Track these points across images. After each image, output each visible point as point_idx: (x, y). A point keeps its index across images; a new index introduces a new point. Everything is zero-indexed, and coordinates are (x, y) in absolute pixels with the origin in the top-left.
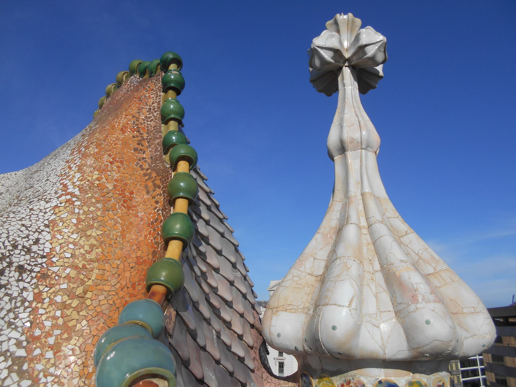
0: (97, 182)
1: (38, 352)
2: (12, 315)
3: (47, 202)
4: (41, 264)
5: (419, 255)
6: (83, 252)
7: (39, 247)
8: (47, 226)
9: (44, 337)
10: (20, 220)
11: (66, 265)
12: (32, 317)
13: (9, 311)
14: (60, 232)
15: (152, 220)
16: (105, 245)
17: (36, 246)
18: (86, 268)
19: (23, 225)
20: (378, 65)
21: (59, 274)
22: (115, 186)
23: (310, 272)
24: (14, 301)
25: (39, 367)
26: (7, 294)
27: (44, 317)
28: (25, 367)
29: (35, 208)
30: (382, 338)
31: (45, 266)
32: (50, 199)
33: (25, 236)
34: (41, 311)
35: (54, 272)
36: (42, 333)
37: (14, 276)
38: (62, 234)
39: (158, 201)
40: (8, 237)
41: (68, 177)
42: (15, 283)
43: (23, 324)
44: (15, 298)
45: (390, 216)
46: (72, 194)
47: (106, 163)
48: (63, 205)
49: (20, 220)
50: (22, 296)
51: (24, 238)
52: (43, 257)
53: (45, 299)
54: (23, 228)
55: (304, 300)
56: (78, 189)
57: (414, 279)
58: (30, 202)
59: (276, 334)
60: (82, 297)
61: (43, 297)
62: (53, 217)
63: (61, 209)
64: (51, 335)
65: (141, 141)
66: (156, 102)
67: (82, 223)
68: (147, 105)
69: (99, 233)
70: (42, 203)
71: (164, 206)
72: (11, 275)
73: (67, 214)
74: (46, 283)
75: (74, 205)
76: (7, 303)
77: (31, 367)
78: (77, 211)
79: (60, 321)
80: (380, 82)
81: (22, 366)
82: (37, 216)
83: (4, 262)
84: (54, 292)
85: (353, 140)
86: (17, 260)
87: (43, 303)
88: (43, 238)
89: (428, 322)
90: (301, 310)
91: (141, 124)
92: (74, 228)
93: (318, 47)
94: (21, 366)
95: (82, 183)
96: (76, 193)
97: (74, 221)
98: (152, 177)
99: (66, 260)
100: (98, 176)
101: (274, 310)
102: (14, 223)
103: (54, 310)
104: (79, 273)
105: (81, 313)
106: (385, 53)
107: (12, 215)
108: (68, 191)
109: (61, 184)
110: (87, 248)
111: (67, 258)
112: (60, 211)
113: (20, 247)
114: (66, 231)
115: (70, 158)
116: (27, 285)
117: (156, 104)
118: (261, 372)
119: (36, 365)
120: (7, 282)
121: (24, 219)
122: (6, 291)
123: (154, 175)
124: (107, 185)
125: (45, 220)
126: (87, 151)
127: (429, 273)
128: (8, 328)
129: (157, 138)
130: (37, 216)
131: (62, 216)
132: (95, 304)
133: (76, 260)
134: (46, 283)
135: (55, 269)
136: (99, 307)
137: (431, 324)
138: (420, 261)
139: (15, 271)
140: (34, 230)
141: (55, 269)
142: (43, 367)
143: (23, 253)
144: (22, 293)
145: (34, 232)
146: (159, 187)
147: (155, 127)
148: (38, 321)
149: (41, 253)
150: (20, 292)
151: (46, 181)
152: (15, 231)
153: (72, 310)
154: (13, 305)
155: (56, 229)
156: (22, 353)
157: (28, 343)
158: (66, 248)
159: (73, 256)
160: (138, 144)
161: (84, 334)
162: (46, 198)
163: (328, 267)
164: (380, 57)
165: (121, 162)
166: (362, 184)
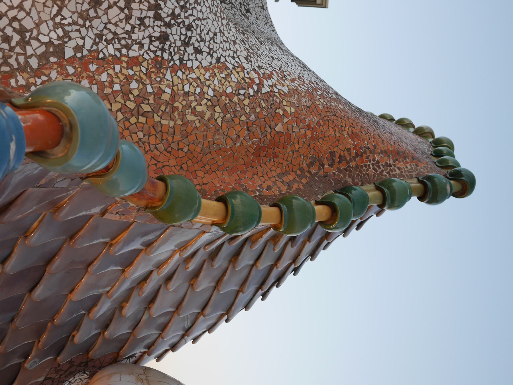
0: (281, 113)
1: (71, 70)
2: (110, 36)
3: (246, 58)
4: (172, 59)
6: (193, 105)
7: (192, 54)
8: (218, 60)
9: (89, 75)
10: (220, 31)
11: (175, 88)
12: (110, 58)
13: (115, 34)
14: (214, 75)
16: (205, 130)
17: (193, 51)
18: (173, 112)
19: (215, 34)
21: (164, 82)
22: (280, 134)
24: (127, 36)
25: (54, 75)
26: (133, 27)
27: (111, 72)
28: (53, 59)
29: (237, 46)
31: (170, 65)
32: (251, 62)
33: (203, 37)
34: (118, 68)
36: (93, 73)
37: (155, 31)
38: (211, 78)
39: (271, 190)
40: (199, 19)
41: (282, 79)
42: (147, 34)
43: (102, 51)
44: (130, 37)
46: (261, 85)
47: (307, 120)
48: (247, 76)
49: (220, 31)
50: (133, 45)
51: (201, 37)
52: (181, 60)
53: (132, 70)
54: (211, 35)
56: (269, 90)
58: (243, 41)
61: (134, 68)
62: (230, 66)
63: (242, 74)
64: (90, 83)
65: (346, 159)
66: (402, 172)
67: (227, 99)
68: (394, 161)
69: (219, 121)
70: (245, 53)
71: (266, 197)
72: (156, 28)
73: (236, 81)
74: (151, 68)
76: (123, 29)
77: (53, 66)
78: (242, 92)
79: (107, 91)
81: (54, 56)
82: (228, 48)
83: (170, 18)
84: (142, 79)
86: (174, 32)
87: (127, 68)
88: (204, 57)
91: (367, 157)
92: (221, 91)
94: (53, 54)
95: (277, 94)
96: (263, 88)
97: (229, 90)
99: (180, 87)
100: (289, 112)
101: (144, 377)
102: (216, 25)
103: (121, 81)
104: (167, 103)
105: (119, 113)
107: (225, 22)
108: (265, 81)
109: (271, 72)
110: (199, 109)
111: (183, 88)
112: (238, 73)
113: (189, 34)
114: (216, 82)
115: (305, 80)
116: (146, 47)
117: (398, 172)
118: (53, 376)
119: (55, 71)
120: (147, 25)
121: (222, 35)
122: (137, 26)
123: (304, 181)
124: (280, 125)
125: (225, 57)
126: (318, 97)
128: (95, 35)
129: (353, 180)
130: (228, 48)
131: (232, 76)
132: (133, 128)
133: (182, 98)
134: (151, 68)
135: (168, 76)
136: (129, 134)
139: (161, 32)
140: (211, 47)
141: (168, 76)
142: (53, 79)
143: (183, 38)
144: (136, 44)
145: (209, 47)
146: (290, 187)
147: (368, 175)
148: (106, 66)
149: (186, 58)
150: (138, 41)
151: (272, 57)
152: (207, 26)
153: (123, 102)
154: (121, 36)
155: (216, 71)
156: (69, 53)
157: (80, 58)
158: (195, 85)
159: (187, 94)
160: (340, 157)
162: (251, 57)
165: (312, 138)
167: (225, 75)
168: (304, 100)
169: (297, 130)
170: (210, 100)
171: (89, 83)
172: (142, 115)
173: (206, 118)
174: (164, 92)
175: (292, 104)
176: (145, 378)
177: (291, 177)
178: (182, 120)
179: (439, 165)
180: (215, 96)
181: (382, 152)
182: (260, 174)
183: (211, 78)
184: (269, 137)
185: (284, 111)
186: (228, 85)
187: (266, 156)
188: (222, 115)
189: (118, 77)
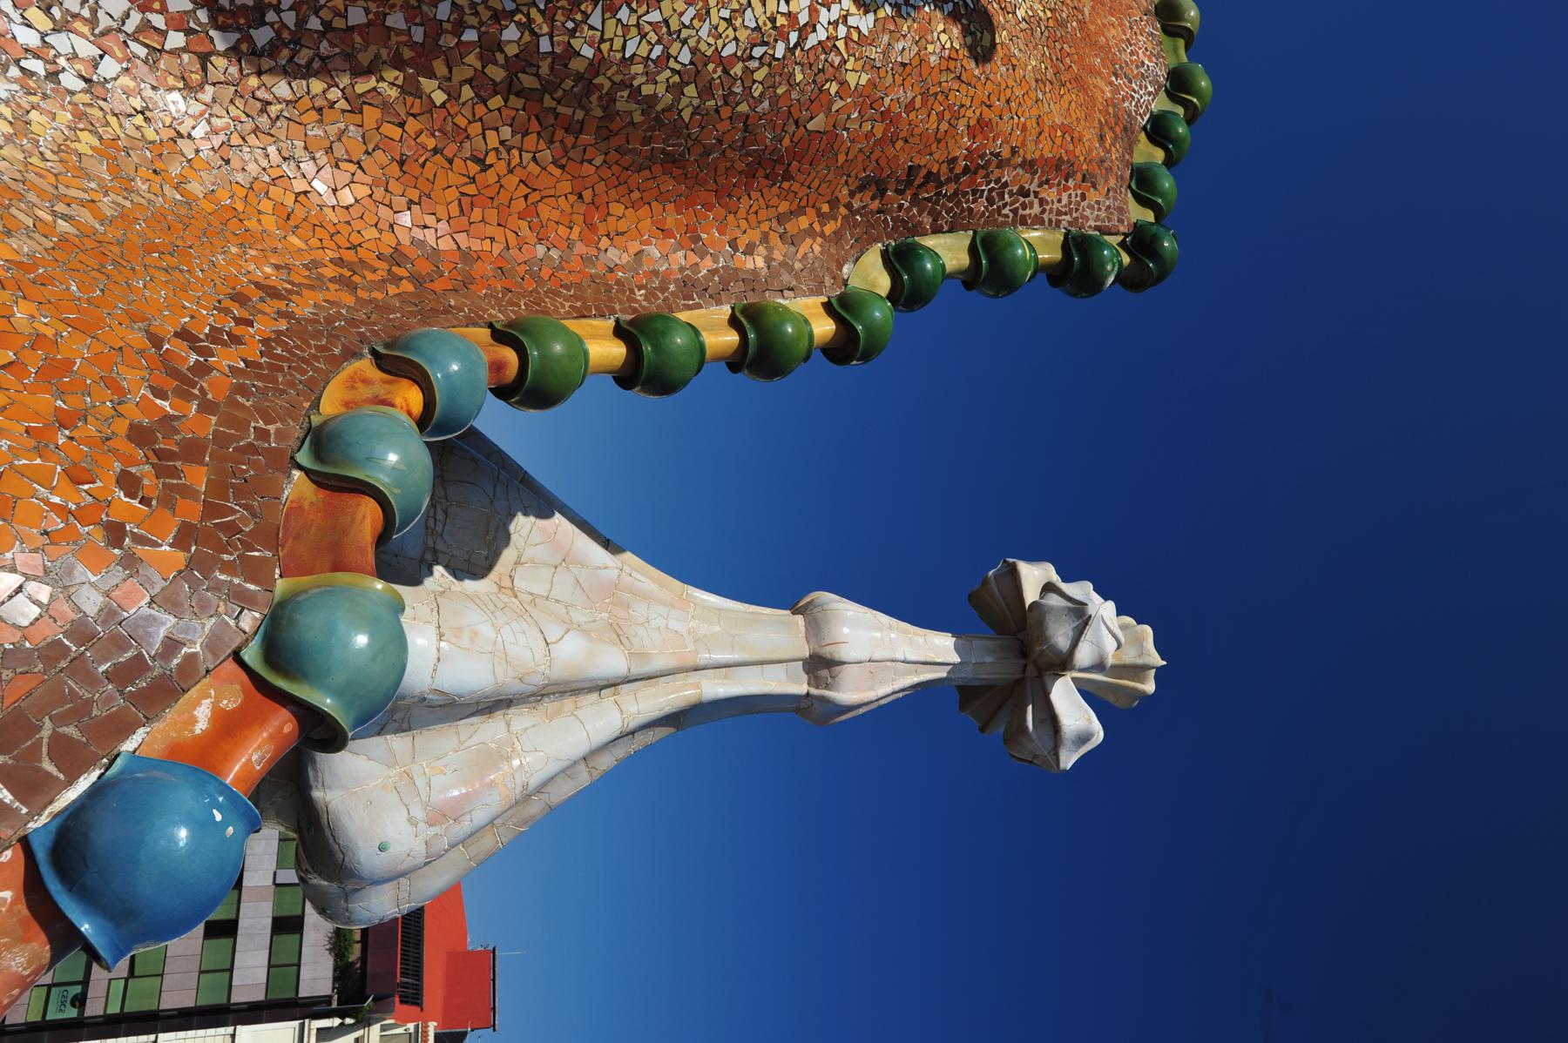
0: (834, 88)
6: (636, 83)
11: (605, 47)
15: (704, 236)
18: (588, 94)
35: (588, 16)
38: (696, 23)
47: (887, 101)
60: (509, 88)
66: (1043, 211)
67: (719, 70)
68: (1040, 186)
69: (686, 115)
75: (776, 41)
78: (757, 52)
79: (449, 41)
84: (530, 20)
90: (431, 544)
91: (986, 176)
95: (841, 45)
97: (729, 50)
98: (823, 225)
99: (618, 44)
104: (579, 77)
108: (823, 11)
114: (703, 33)
117: (1036, 209)
123: (829, 228)
141: (596, 20)
147: (970, 210)
153: (479, 66)
161: (409, 99)
167: (733, 11)
168: (899, 46)
169: (853, 126)
170: (678, 72)
171: (407, 21)
172: (518, 95)
173: (659, 108)
174: (578, 54)
175: (869, 65)
177: (804, 222)
178: (605, 109)
179: (1133, 186)
180: (691, 63)
181: (1022, 165)
182: (742, 212)
183: (696, 23)
184: (786, 142)
185: (843, 83)
186: (732, 35)
187: (767, 177)
188: (696, 102)
189: (477, 14)
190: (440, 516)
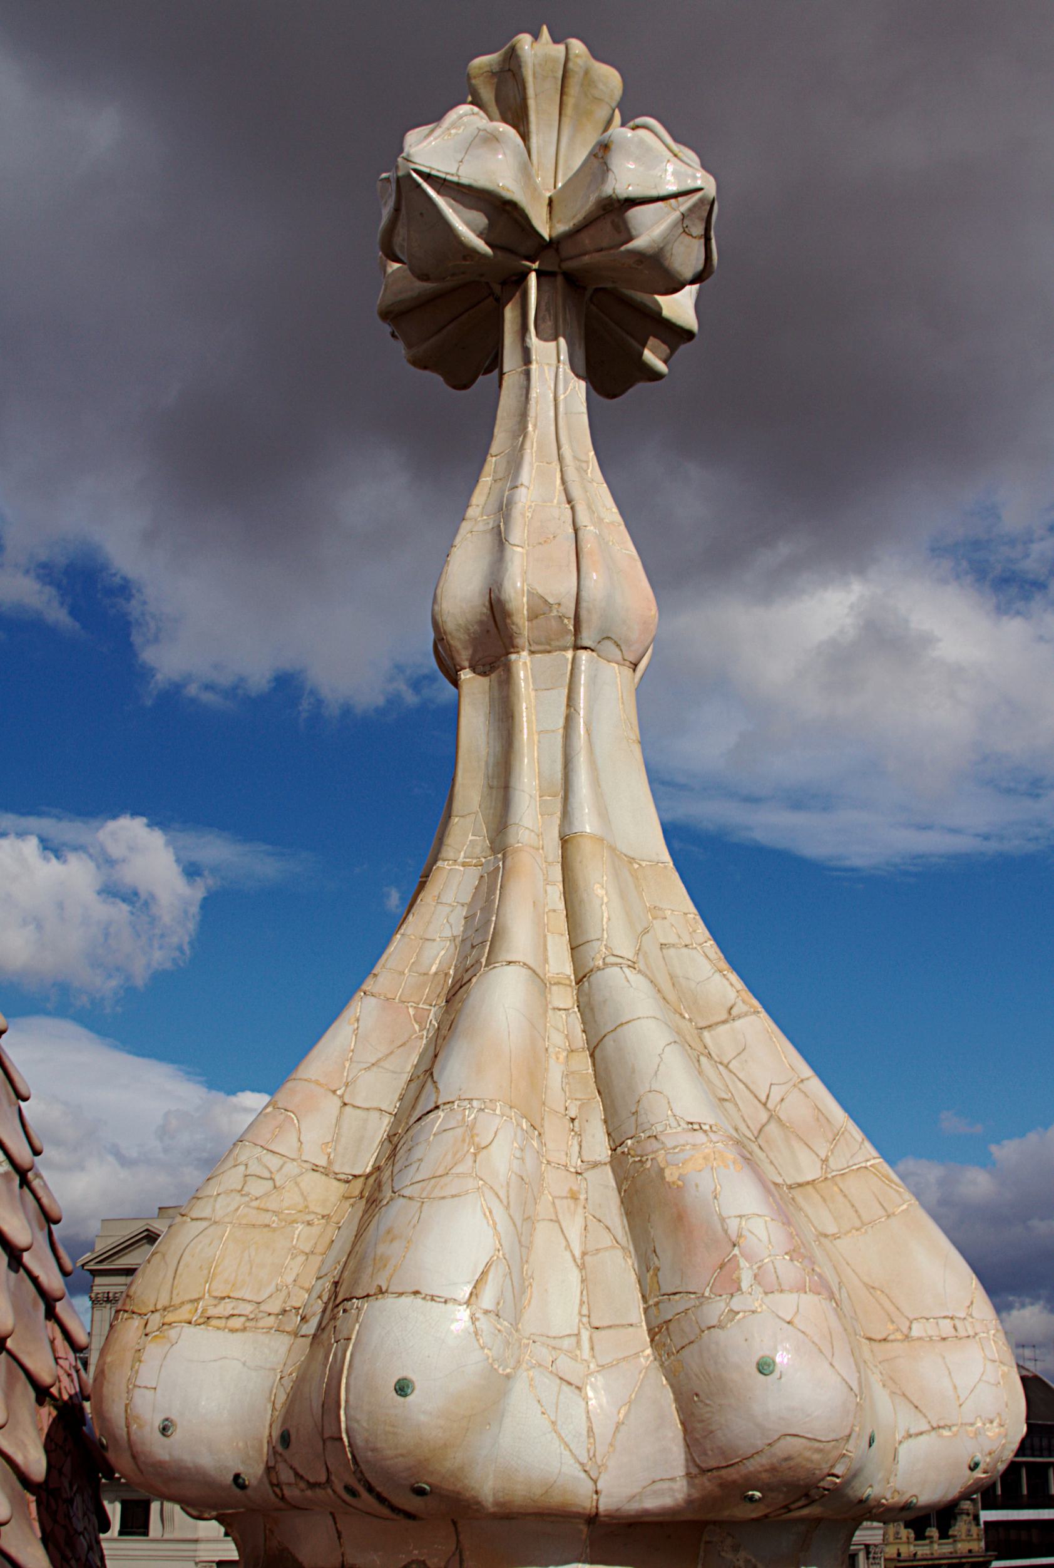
5: (770, 1105)
20: (674, 286)
23: (322, 1162)
30: (590, 1430)
45: (672, 939)
55: (289, 1279)
57: (736, 1201)
59: (157, 1423)
80: (684, 348)
85: (540, 608)
89: (765, 1367)
93: (427, 177)
101: (155, 1320)
106: (707, 240)
127: (800, 1180)
137: (776, 1374)
138: (773, 1128)
163: (395, 1145)
164: (687, 257)
166: (566, 799)
176: (157, 1315)
190: (226, 1308)
